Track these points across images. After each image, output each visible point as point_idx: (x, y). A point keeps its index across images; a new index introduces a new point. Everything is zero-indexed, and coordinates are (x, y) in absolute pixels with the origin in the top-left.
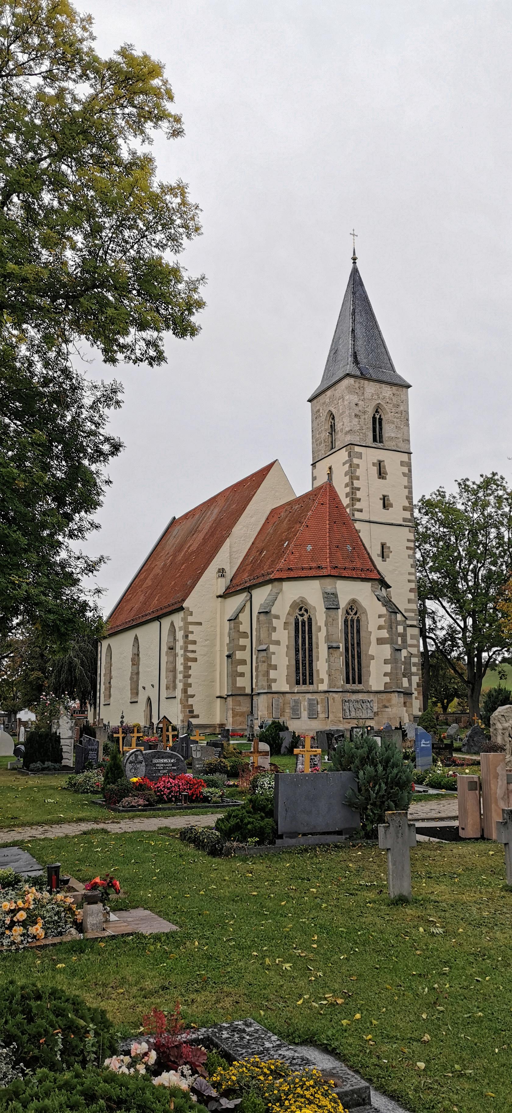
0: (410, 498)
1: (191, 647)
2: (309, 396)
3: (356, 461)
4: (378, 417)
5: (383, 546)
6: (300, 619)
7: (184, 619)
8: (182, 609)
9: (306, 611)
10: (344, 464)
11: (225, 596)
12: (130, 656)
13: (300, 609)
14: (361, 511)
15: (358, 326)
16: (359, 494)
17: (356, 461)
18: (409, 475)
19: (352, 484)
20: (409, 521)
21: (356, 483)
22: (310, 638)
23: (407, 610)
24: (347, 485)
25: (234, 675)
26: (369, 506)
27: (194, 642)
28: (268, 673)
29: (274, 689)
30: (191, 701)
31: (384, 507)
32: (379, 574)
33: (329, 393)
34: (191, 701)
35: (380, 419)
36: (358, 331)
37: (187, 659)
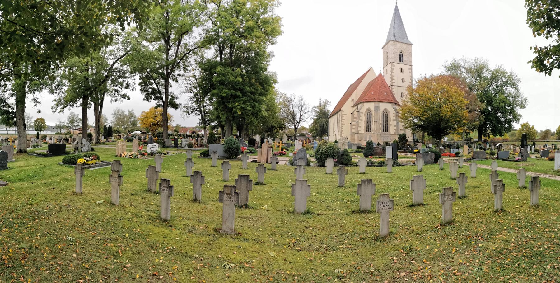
0: (411, 80)
3: (393, 67)
8: (340, 110)
16: (394, 78)
17: (393, 67)
18: (411, 73)
21: (393, 74)
37: (342, 124)
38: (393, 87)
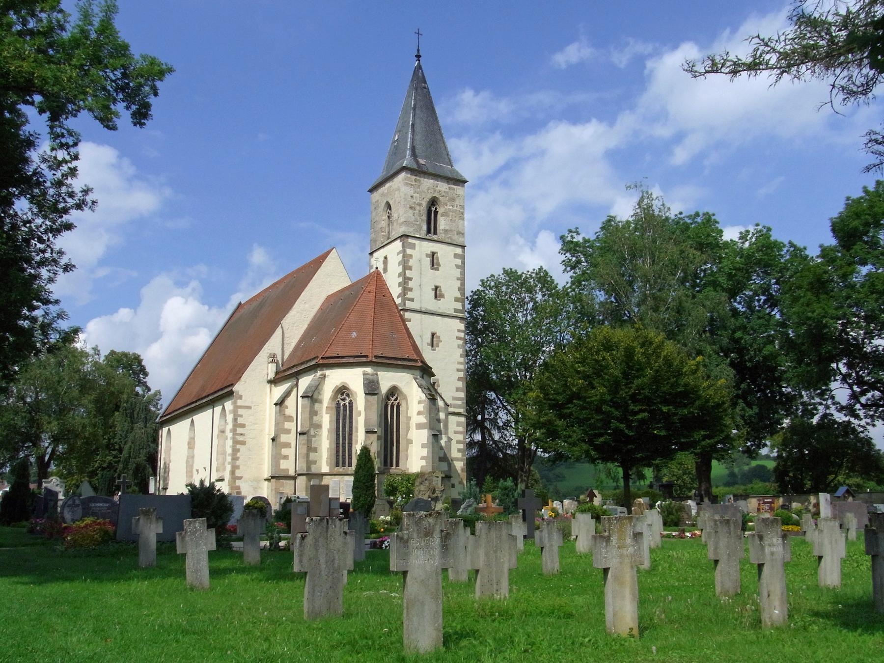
1: (239, 430)
2: (370, 187)
3: (409, 251)
4: (433, 209)
5: (433, 335)
6: (342, 403)
7: (234, 403)
8: (231, 393)
9: (348, 395)
10: (398, 254)
11: (274, 382)
12: (186, 439)
13: (342, 394)
14: (412, 300)
15: (418, 121)
16: (411, 284)
17: (409, 251)
18: (462, 267)
19: (405, 274)
20: (461, 312)
22: (351, 423)
23: (455, 399)
24: (400, 275)
25: (277, 458)
26: (422, 298)
27: (243, 426)
28: (308, 456)
29: (314, 470)
30: (238, 483)
31: (436, 297)
32: (423, 362)
33: (387, 185)
34: (238, 483)
35: (436, 213)
36: (418, 128)
37: (235, 442)
38: (407, 315)
